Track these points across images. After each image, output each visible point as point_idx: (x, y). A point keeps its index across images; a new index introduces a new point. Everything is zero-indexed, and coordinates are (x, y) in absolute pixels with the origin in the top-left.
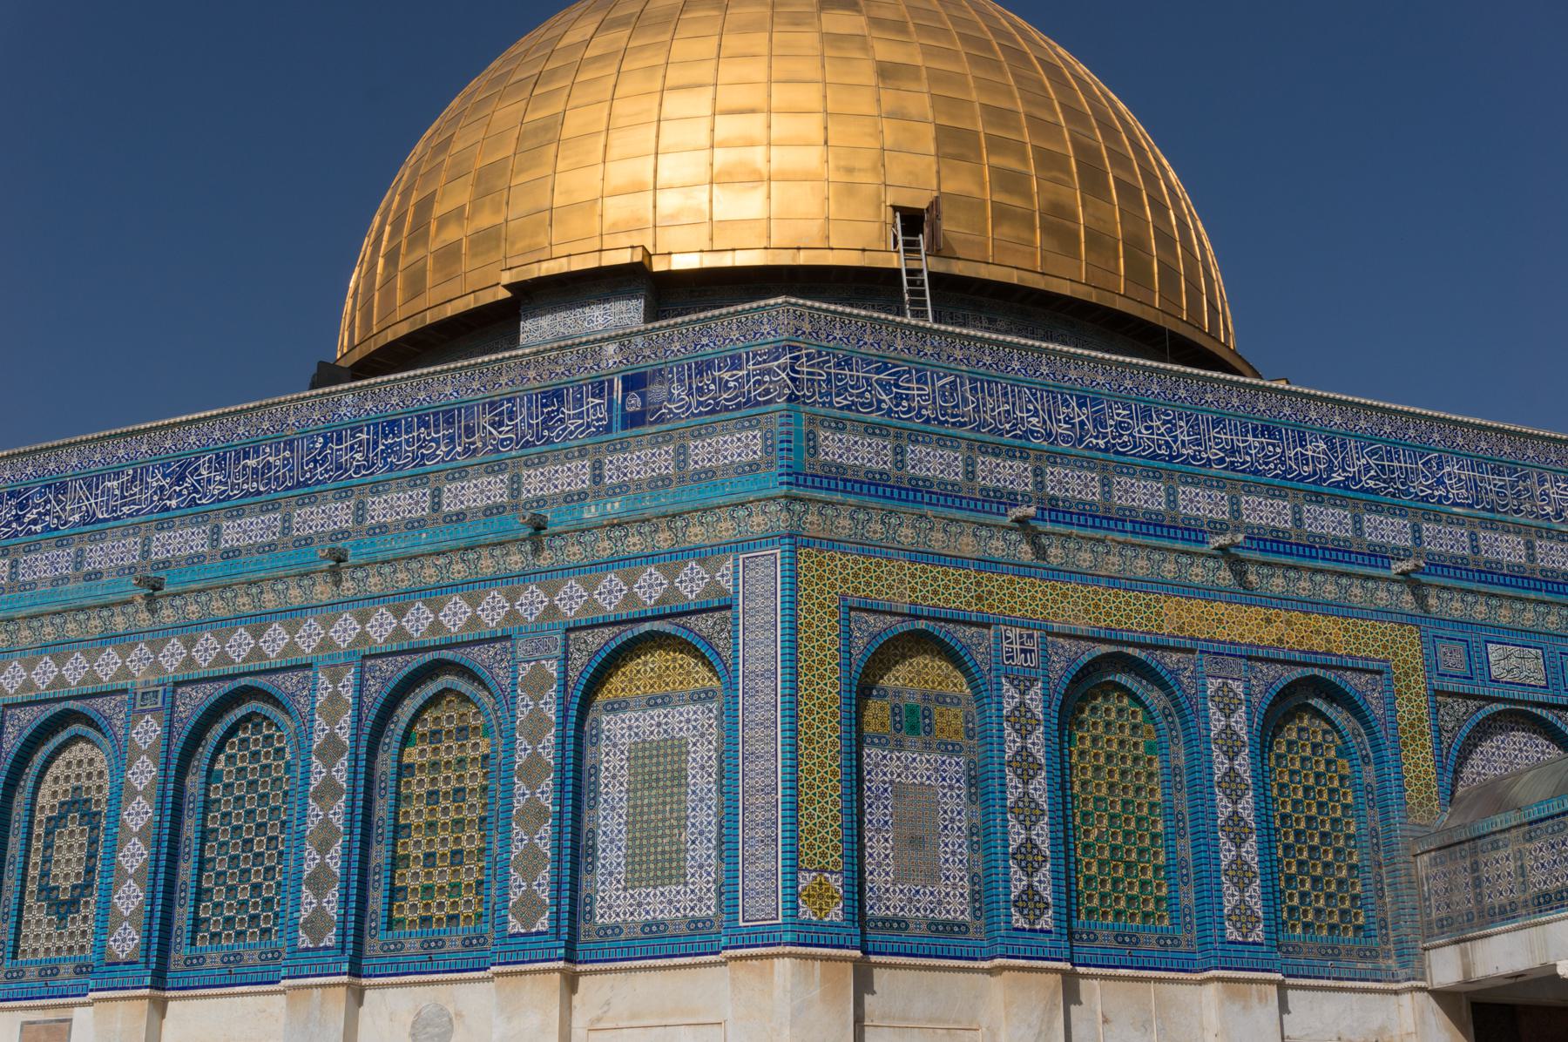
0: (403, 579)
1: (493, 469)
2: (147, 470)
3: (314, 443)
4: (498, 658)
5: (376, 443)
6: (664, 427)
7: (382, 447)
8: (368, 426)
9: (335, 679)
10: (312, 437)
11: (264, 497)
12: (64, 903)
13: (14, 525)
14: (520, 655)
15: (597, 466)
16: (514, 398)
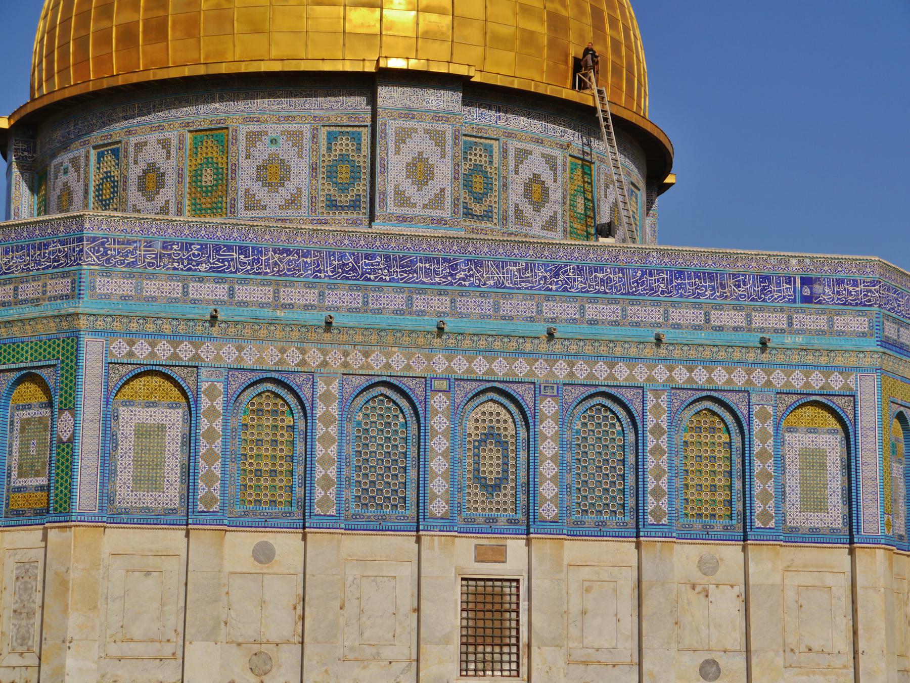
0: (693, 354)
1: (736, 308)
2: (535, 266)
3: (636, 273)
4: (741, 400)
5: (672, 281)
6: (823, 307)
7: (675, 284)
8: (667, 271)
9: (657, 397)
10: (634, 269)
11: (608, 296)
12: (491, 486)
13: (449, 278)
14: (753, 401)
15: (790, 319)
16: (746, 275)
